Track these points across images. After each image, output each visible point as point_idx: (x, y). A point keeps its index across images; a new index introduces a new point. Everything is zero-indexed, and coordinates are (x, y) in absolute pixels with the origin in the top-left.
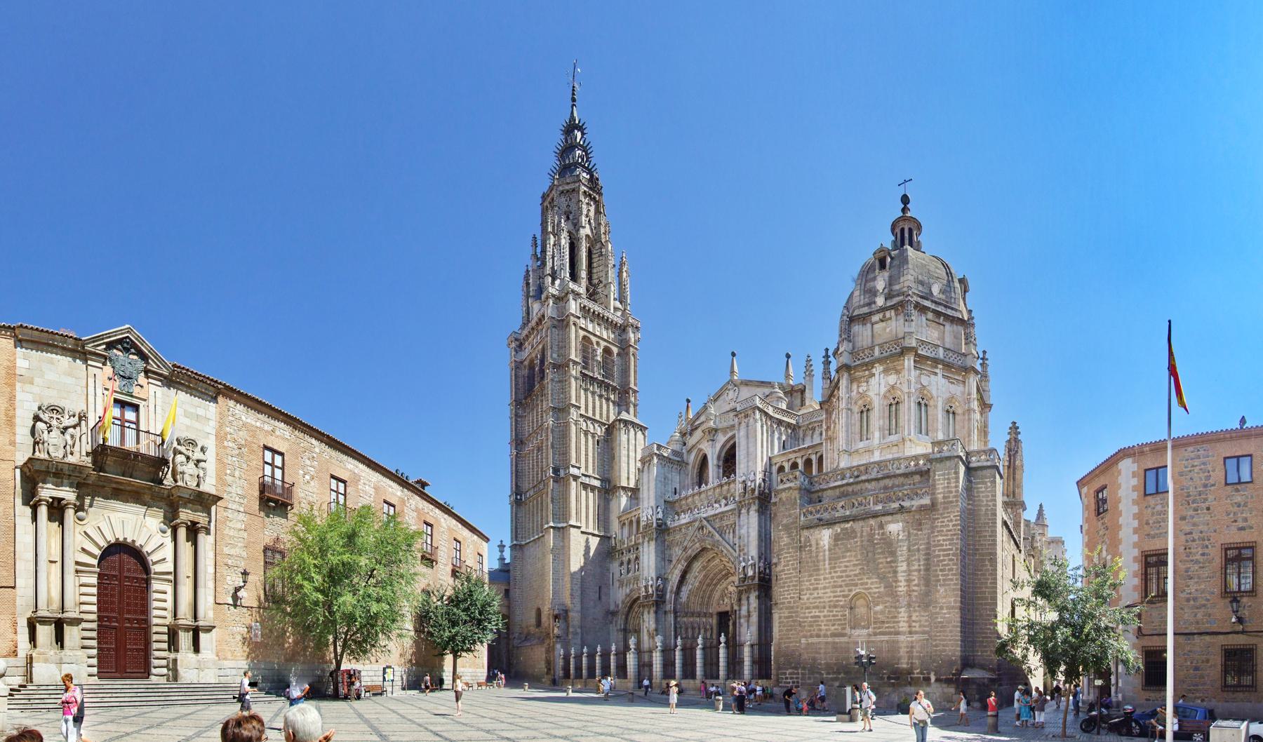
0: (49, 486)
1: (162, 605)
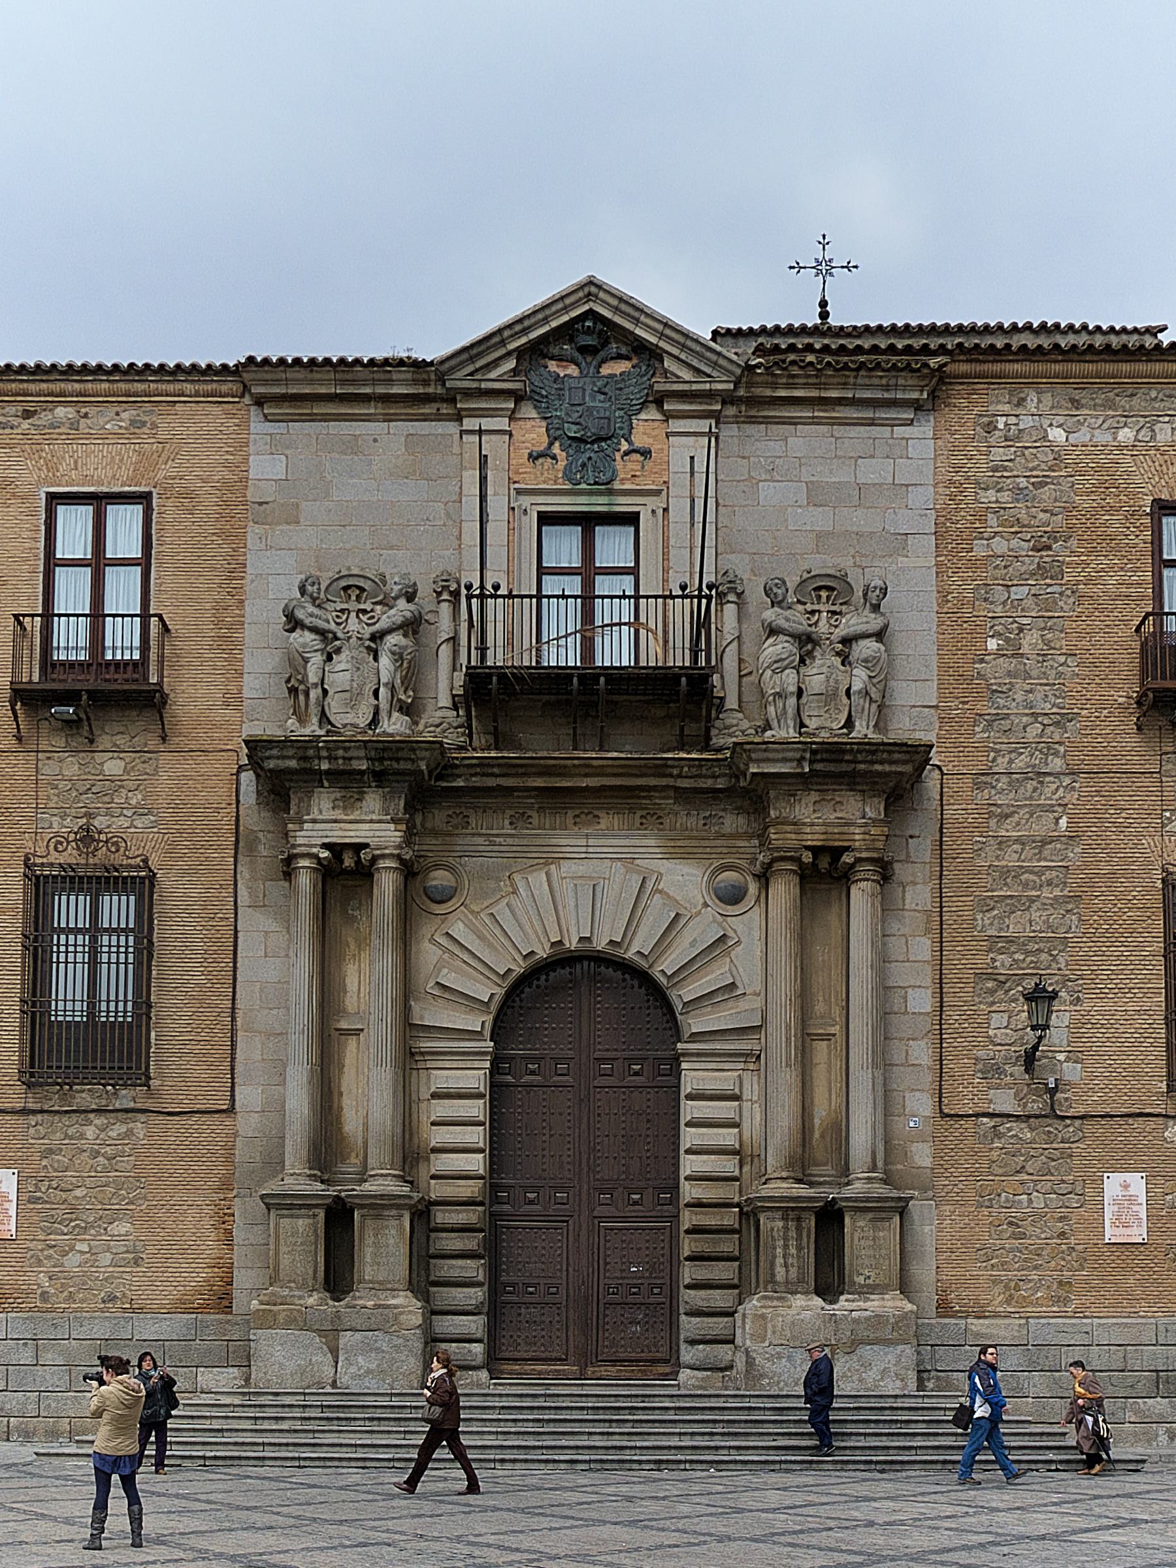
1: (729, 1122)
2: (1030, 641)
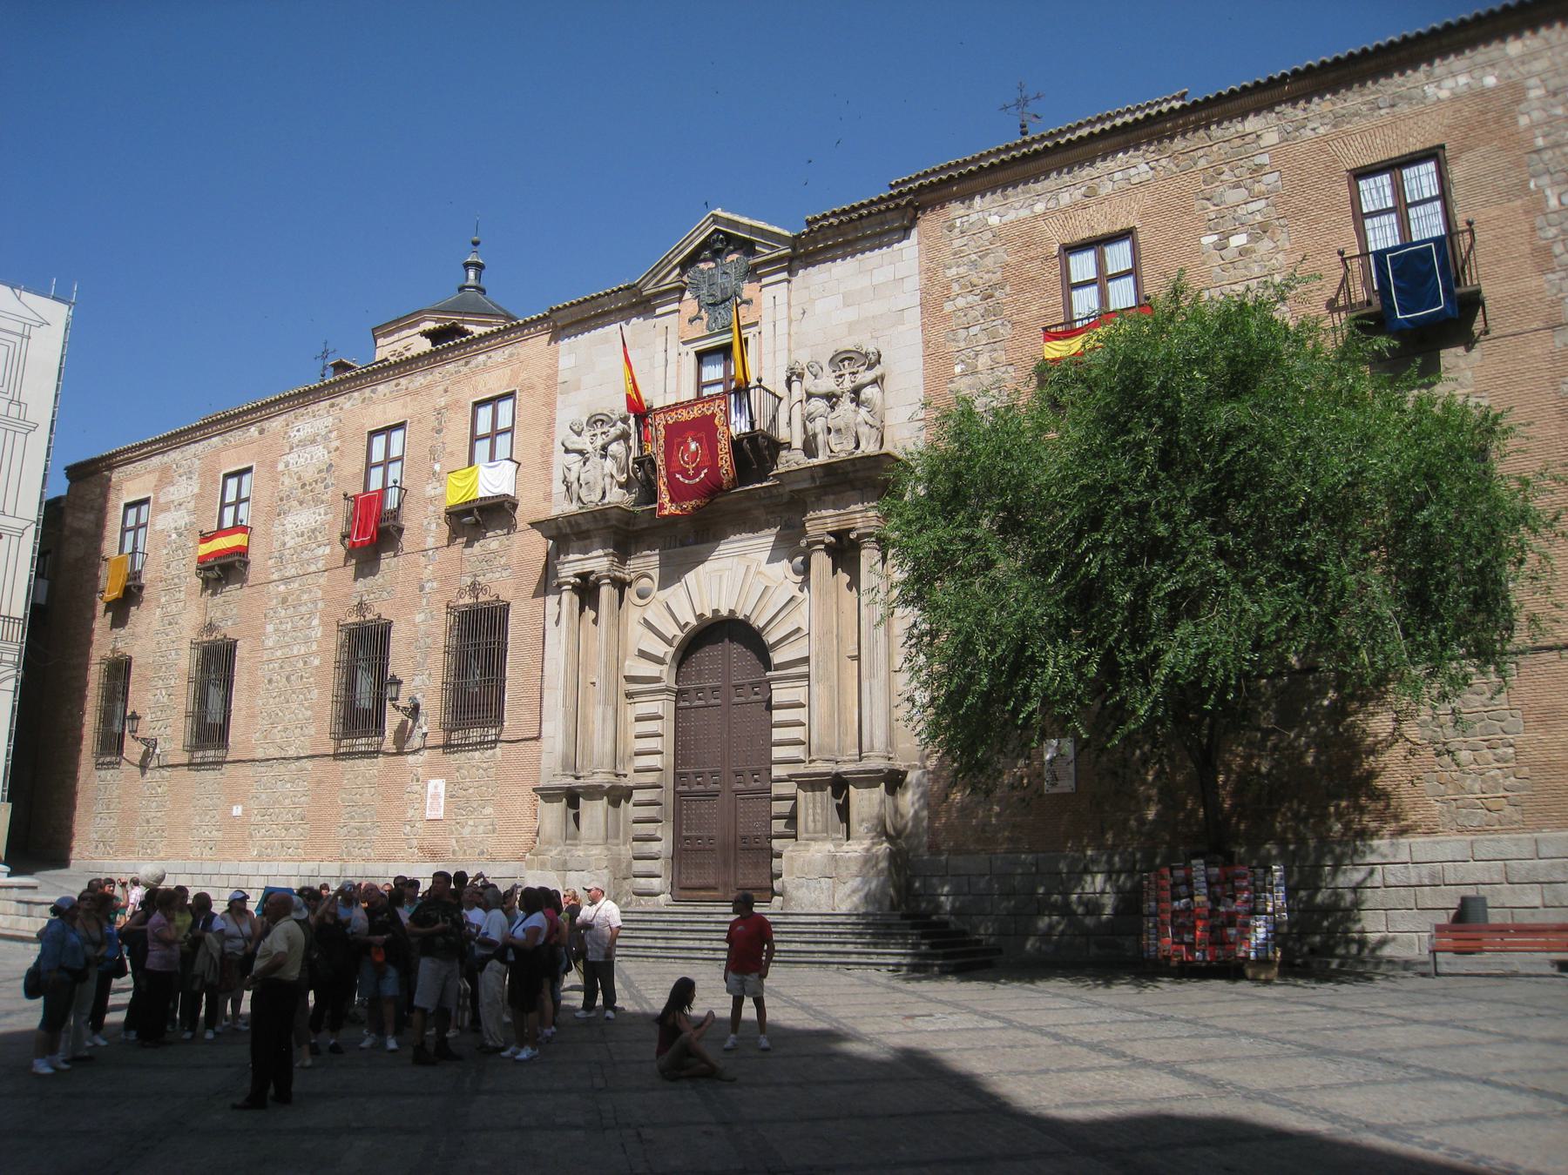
0: (572, 557)
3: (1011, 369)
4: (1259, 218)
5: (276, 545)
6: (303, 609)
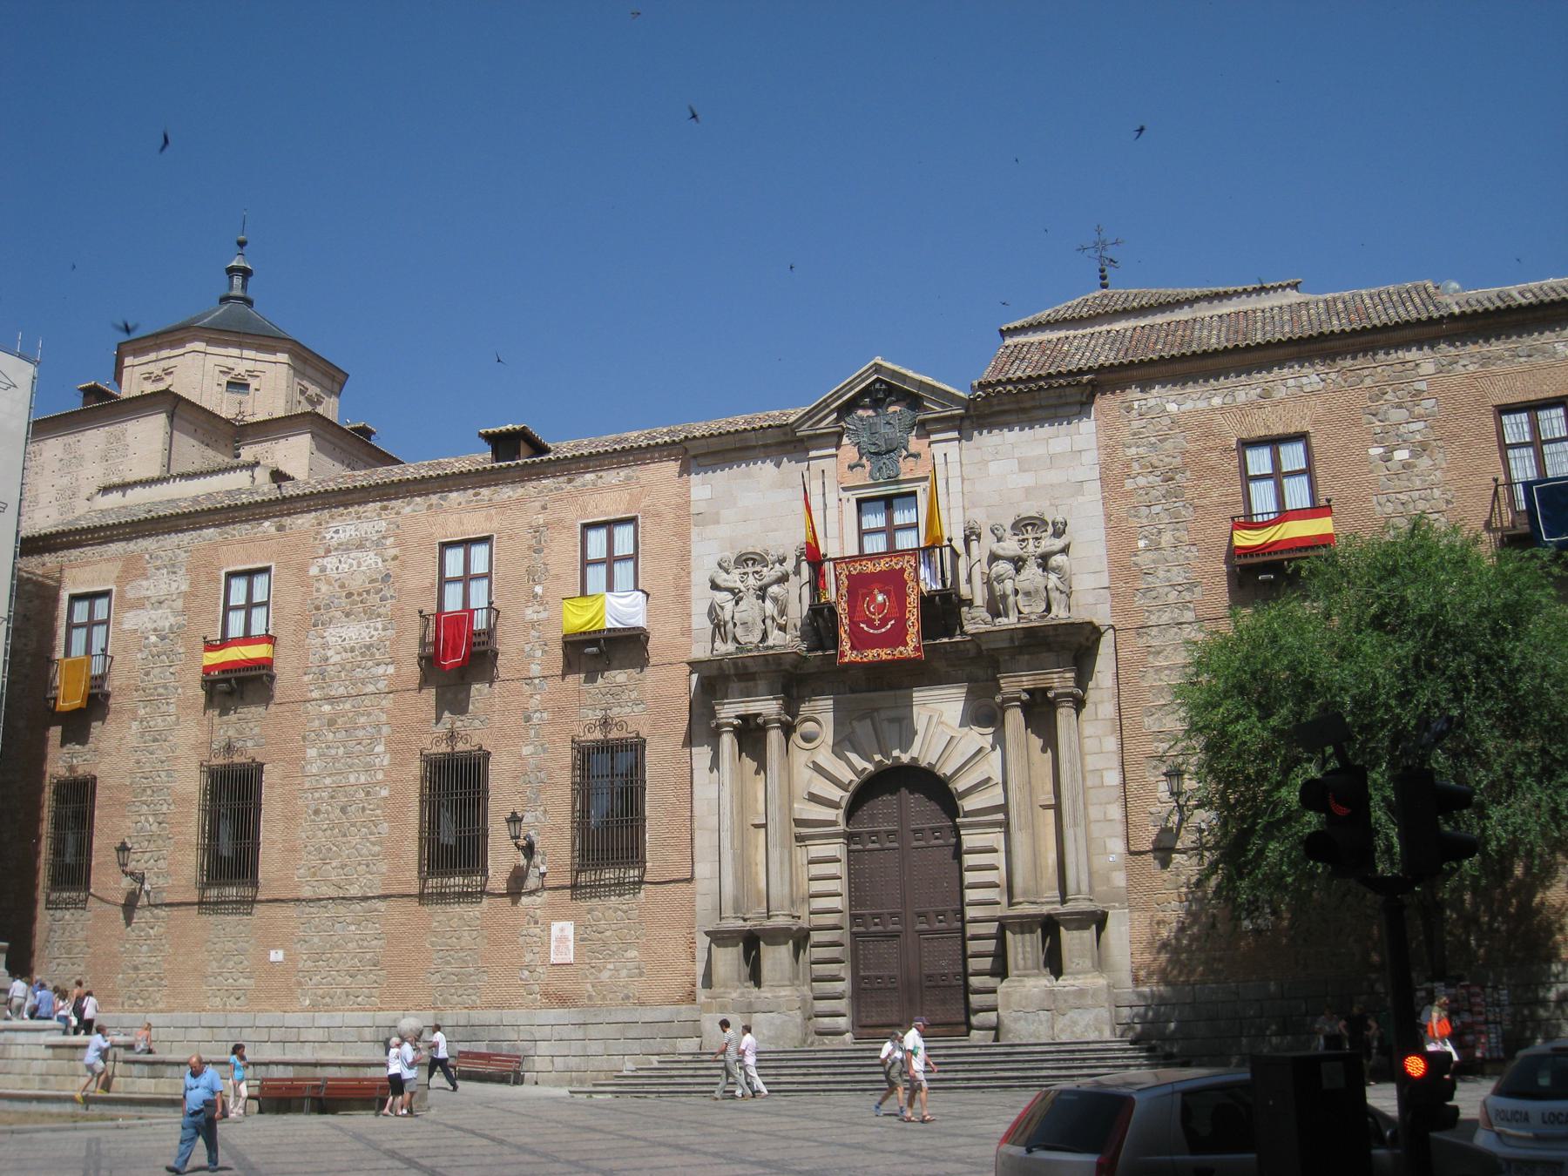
2: (1167, 539)
3: (1194, 549)
4: (1419, 437)
5: (314, 659)
6: (360, 734)
